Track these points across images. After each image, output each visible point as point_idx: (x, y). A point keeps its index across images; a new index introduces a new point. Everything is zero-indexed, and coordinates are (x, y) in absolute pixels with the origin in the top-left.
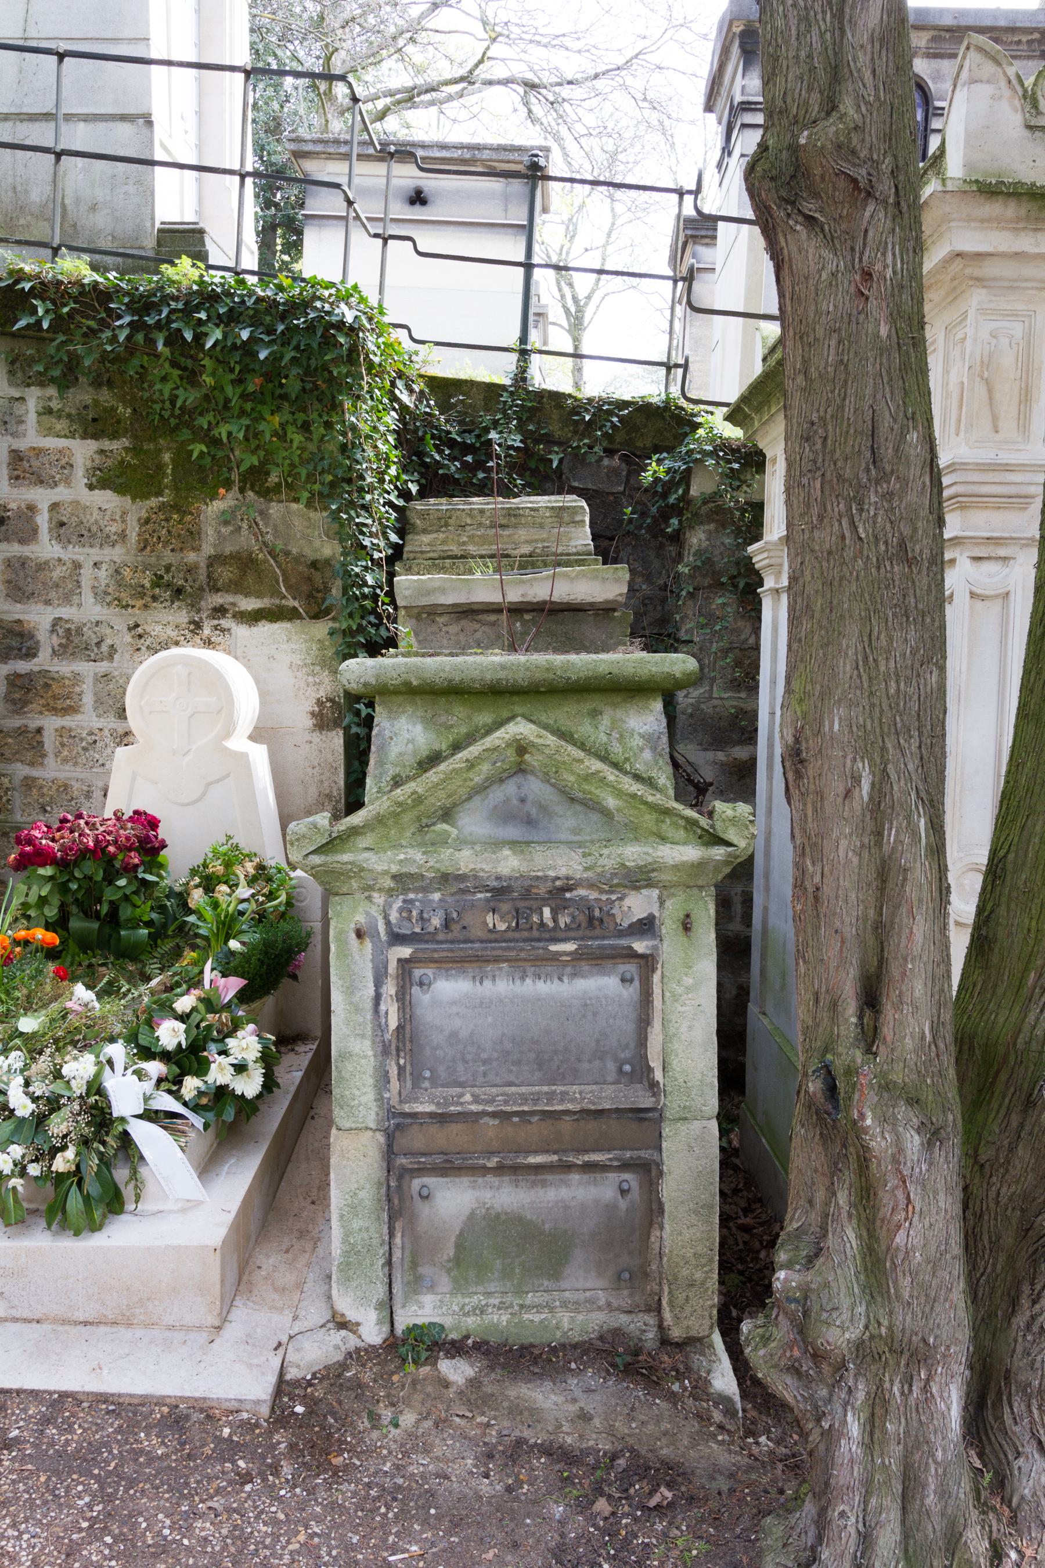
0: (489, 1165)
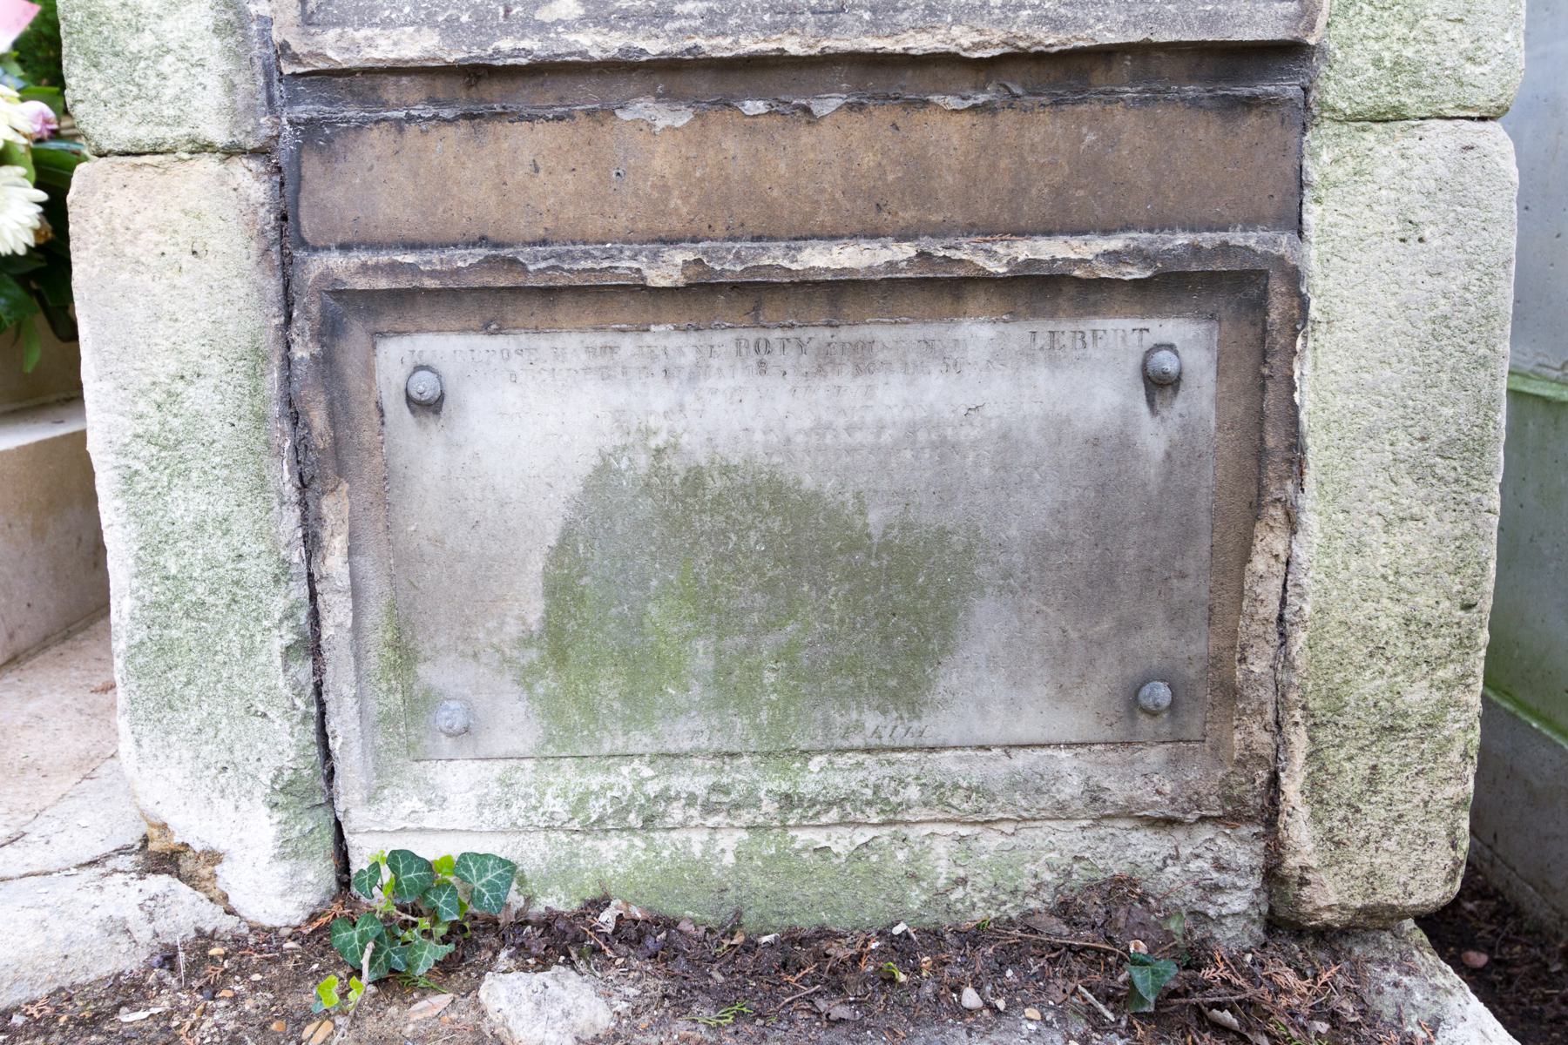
0: (656, 278)
